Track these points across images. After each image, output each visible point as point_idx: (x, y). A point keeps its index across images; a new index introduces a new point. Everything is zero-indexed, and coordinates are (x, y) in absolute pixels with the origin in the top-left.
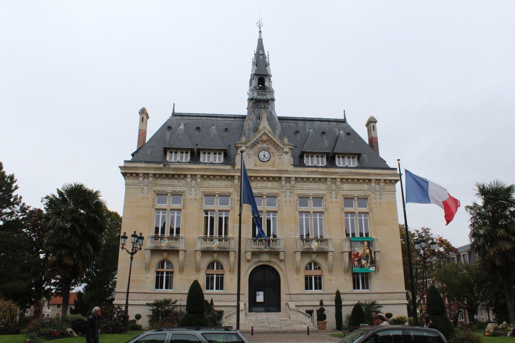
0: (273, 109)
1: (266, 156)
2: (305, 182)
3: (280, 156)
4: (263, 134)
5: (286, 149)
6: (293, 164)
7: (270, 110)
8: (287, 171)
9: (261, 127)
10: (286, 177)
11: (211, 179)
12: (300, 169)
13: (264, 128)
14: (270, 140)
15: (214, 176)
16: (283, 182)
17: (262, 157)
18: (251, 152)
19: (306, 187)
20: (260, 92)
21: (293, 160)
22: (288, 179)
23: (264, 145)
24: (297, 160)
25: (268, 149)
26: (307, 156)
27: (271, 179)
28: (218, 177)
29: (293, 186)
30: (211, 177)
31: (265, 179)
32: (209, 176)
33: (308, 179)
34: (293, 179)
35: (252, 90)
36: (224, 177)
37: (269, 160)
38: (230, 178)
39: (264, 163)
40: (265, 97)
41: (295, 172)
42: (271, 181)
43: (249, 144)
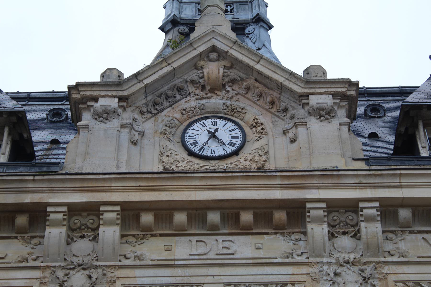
3: (291, 135)
4: (205, 56)
8: (331, 176)
10: (333, 206)
16: (318, 231)
17: (203, 138)
18: (148, 126)
22: (344, 215)
23: (214, 102)
25: (233, 111)
27: (247, 217)
29: (374, 249)
37: (236, 153)
38: (22, 220)
42: (247, 231)
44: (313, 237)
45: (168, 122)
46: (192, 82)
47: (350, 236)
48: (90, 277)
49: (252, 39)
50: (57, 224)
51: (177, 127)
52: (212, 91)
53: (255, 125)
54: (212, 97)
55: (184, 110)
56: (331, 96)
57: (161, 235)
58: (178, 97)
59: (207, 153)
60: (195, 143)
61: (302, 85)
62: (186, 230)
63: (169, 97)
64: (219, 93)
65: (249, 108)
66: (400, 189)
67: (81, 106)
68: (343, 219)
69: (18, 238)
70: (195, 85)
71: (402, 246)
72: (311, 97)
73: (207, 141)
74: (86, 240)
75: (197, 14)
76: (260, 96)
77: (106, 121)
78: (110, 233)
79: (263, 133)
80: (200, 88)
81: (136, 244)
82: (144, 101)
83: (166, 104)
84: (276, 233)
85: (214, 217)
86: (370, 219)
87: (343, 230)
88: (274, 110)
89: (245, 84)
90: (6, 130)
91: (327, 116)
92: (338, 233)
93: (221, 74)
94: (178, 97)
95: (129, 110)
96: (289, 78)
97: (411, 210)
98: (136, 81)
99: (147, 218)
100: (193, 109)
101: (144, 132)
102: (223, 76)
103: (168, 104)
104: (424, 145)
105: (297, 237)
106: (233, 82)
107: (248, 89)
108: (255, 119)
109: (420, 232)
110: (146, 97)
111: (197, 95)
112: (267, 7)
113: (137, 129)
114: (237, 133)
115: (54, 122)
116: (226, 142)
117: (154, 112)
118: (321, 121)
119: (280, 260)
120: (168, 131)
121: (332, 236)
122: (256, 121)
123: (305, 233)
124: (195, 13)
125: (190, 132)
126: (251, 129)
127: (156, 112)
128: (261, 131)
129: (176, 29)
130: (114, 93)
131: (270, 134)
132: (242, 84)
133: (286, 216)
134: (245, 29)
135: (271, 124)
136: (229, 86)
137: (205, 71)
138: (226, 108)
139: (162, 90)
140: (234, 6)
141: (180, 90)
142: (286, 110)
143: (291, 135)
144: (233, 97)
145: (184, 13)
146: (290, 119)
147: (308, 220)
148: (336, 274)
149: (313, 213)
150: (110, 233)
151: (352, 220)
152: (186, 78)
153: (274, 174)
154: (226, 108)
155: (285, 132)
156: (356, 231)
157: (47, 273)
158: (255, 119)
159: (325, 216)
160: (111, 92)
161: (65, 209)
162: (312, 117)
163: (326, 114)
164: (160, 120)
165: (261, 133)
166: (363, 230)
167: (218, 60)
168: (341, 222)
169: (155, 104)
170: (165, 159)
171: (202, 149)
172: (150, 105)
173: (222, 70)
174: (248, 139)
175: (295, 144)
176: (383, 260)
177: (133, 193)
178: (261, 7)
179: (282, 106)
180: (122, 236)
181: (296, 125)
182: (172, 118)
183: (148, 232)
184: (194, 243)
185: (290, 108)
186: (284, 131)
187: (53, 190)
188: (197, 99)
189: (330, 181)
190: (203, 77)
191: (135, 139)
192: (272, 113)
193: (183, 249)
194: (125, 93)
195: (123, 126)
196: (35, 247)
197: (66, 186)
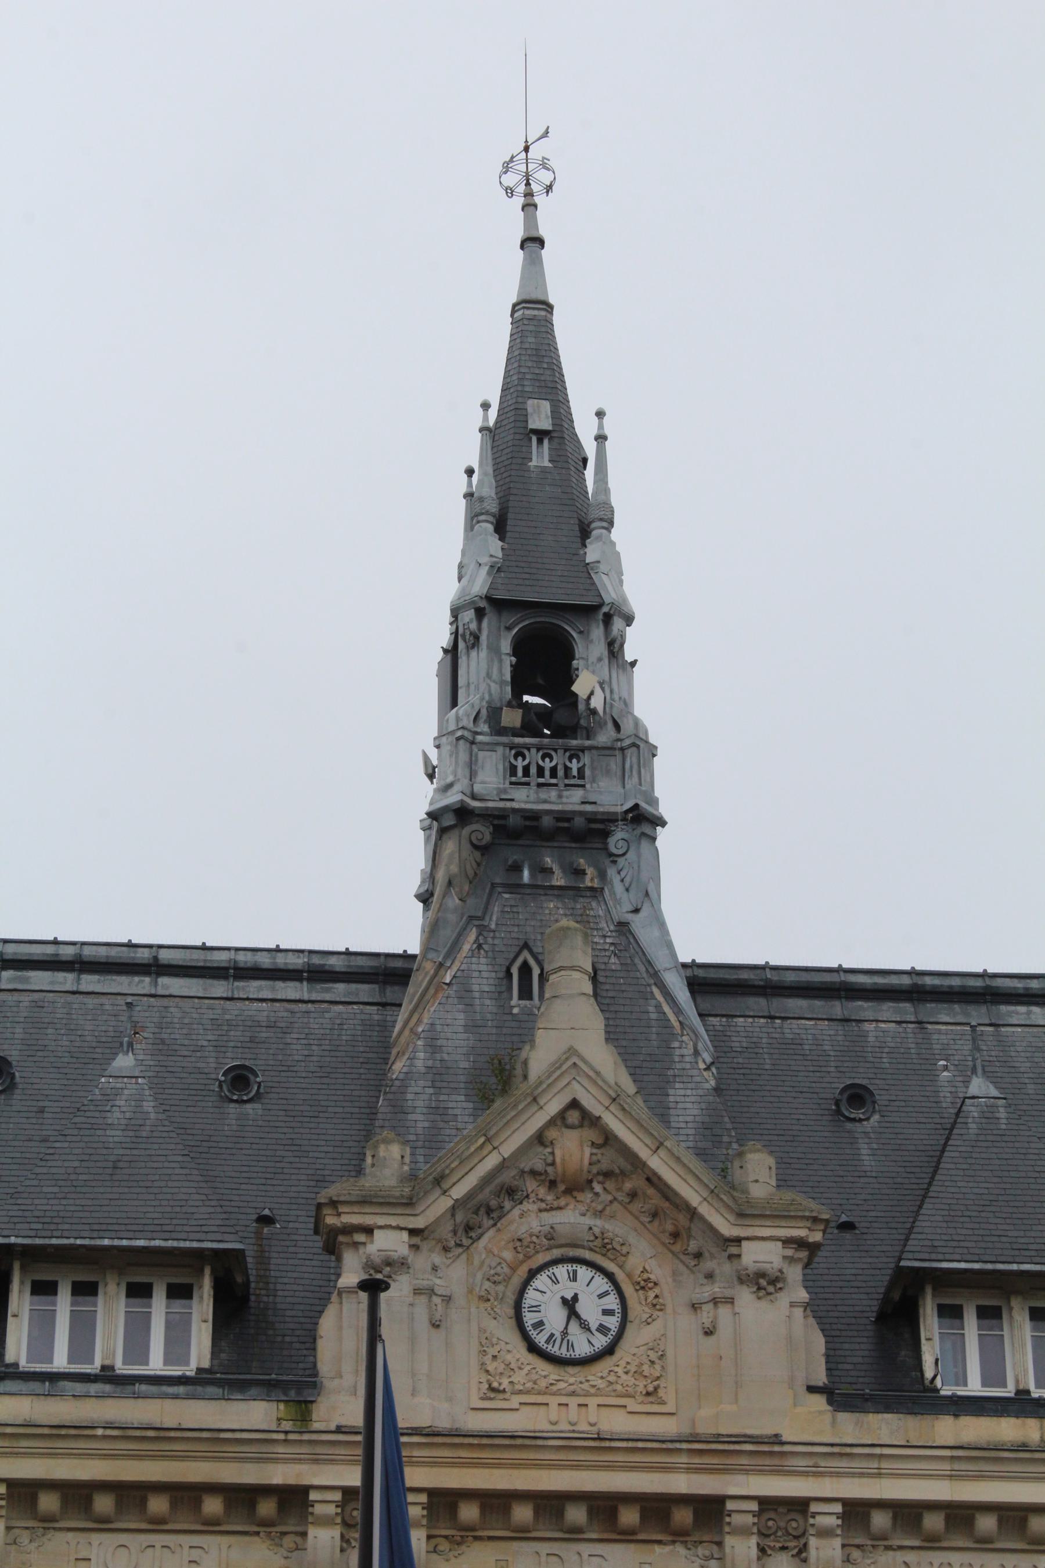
0: (647, 896)
1: (590, 1310)
3: (706, 1315)
5: (762, 1253)
6: (821, 1378)
7: (621, 911)
8: (770, 1451)
10: (767, 1504)
11: (103, 1524)
12: (884, 1427)
13: (571, 1061)
14: (619, 1173)
15: (131, 1495)
17: (555, 1318)
18: (455, 1275)
20: (534, 757)
21: (819, 1343)
23: (572, 1218)
24: (861, 1348)
25: (606, 1247)
26: (951, 1313)
27: (629, 1516)
28: (158, 1505)
30: (104, 1504)
31: (576, 1514)
32: (77, 1495)
33: (960, 1516)
34: (828, 1517)
35: (459, 739)
36: (213, 1506)
37: (609, 1351)
38: (267, 1508)
39: (572, 1376)
40: (572, 800)
42: (627, 1536)
43: (435, 1208)
44: (733, 1561)
45: (492, 1272)
46: (534, 1173)
47: (790, 1554)
49: (623, 874)
50: (326, 1521)
51: (507, 1279)
52: (568, 1192)
53: (644, 1285)
54: (567, 1205)
55: (520, 1240)
56: (780, 1244)
57: (491, 1538)
58: (507, 1204)
60: (539, 1325)
61: (731, 1218)
62: (529, 1532)
63: (492, 1211)
64: (580, 1196)
65: (632, 1239)
66: (877, 1480)
67: (341, 1238)
68: (782, 1524)
69: (262, 1534)
70: (538, 1178)
72: (744, 1243)
75: (507, 785)
76: (655, 1215)
80: (547, 1184)
81: (451, 1554)
82: (449, 1227)
83: (487, 1222)
84: (674, 1542)
86: (825, 1533)
87: (780, 1545)
88: (677, 1248)
90: (207, 1271)
91: (771, 1289)
92: (773, 1548)
93: (586, 1162)
94: (507, 1204)
95: (425, 1246)
96: (709, 1199)
97: (891, 1515)
98: (437, 1192)
99: (469, 1512)
100: (534, 1239)
101: (450, 1297)
102: (590, 1164)
103: (491, 1222)
104: (929, 1335)
105: (707, 1553)
106: (607, 1175)
107: (633, 1195)
108: (644, 1271)
109: (901, 1548)
110: (453, 1215)
111: (542, 1200)
112: (654, 755)
114: (612, 1302)
115: (236, 1101)
116: (594, 1326)
117: (466, 1242)
118: (759, 1298)
120: (493, 1293)
121: (762, 1550)
122: (645, 1276)
123: (720, 1544)
124: (505, 778)
125: (531, 1296)
126: (637, 1290)
127: (470, 1241)
128: (655, 1302)
129: (466, 831)
131: (669, 1309)
132: (623, 1182)
133: (691, 1516)
134: (606, 834)
135: (670, 1280)
136: (599, 1183)
137: (558, 1153)
138: (592, 1238)
139: (480, 1197)
140: (586, 759)
141: (511, 1192)
142: (698, 1255)
144: (604, 1209)
145: (480, 777)
146: (706, 1277)
147: (727, 1529)
151: (795, 1529)
152: (522, 1166)
153: (678, 1445)
154: (592, 1238)
156: (801, 1546)
158: (644, 1271)
159: (754, 1524)
160: (396, 1217)
161: (337, 1496)
162: (745, 1287)
163: (769, 1283)
164: (476, 1262)
165: (654, 1305)
166: (813, 1553)
167: (581, 1126)
168: (779, 1528)
169: (468, 1228)
173: (588, 1151)
174: (631, 1316)
175: (712, 1339)
177: (448, 1470)
178: (642, 770)
179: (693, 1246)
181: (715, 1301)
182: (498, 1260)
184: (543, 1558)
185: (707, 1254)
186: (693, 1305)
187: (317, 1460)
188: (540, 1211)
189: (768, 1461)
190: (553, 1164)
191: (437, 1317)
192: (673, 1253)
194: (419, 1223)
195: (417, 1291)
196: (289, 1554)
197: (337, 1452)
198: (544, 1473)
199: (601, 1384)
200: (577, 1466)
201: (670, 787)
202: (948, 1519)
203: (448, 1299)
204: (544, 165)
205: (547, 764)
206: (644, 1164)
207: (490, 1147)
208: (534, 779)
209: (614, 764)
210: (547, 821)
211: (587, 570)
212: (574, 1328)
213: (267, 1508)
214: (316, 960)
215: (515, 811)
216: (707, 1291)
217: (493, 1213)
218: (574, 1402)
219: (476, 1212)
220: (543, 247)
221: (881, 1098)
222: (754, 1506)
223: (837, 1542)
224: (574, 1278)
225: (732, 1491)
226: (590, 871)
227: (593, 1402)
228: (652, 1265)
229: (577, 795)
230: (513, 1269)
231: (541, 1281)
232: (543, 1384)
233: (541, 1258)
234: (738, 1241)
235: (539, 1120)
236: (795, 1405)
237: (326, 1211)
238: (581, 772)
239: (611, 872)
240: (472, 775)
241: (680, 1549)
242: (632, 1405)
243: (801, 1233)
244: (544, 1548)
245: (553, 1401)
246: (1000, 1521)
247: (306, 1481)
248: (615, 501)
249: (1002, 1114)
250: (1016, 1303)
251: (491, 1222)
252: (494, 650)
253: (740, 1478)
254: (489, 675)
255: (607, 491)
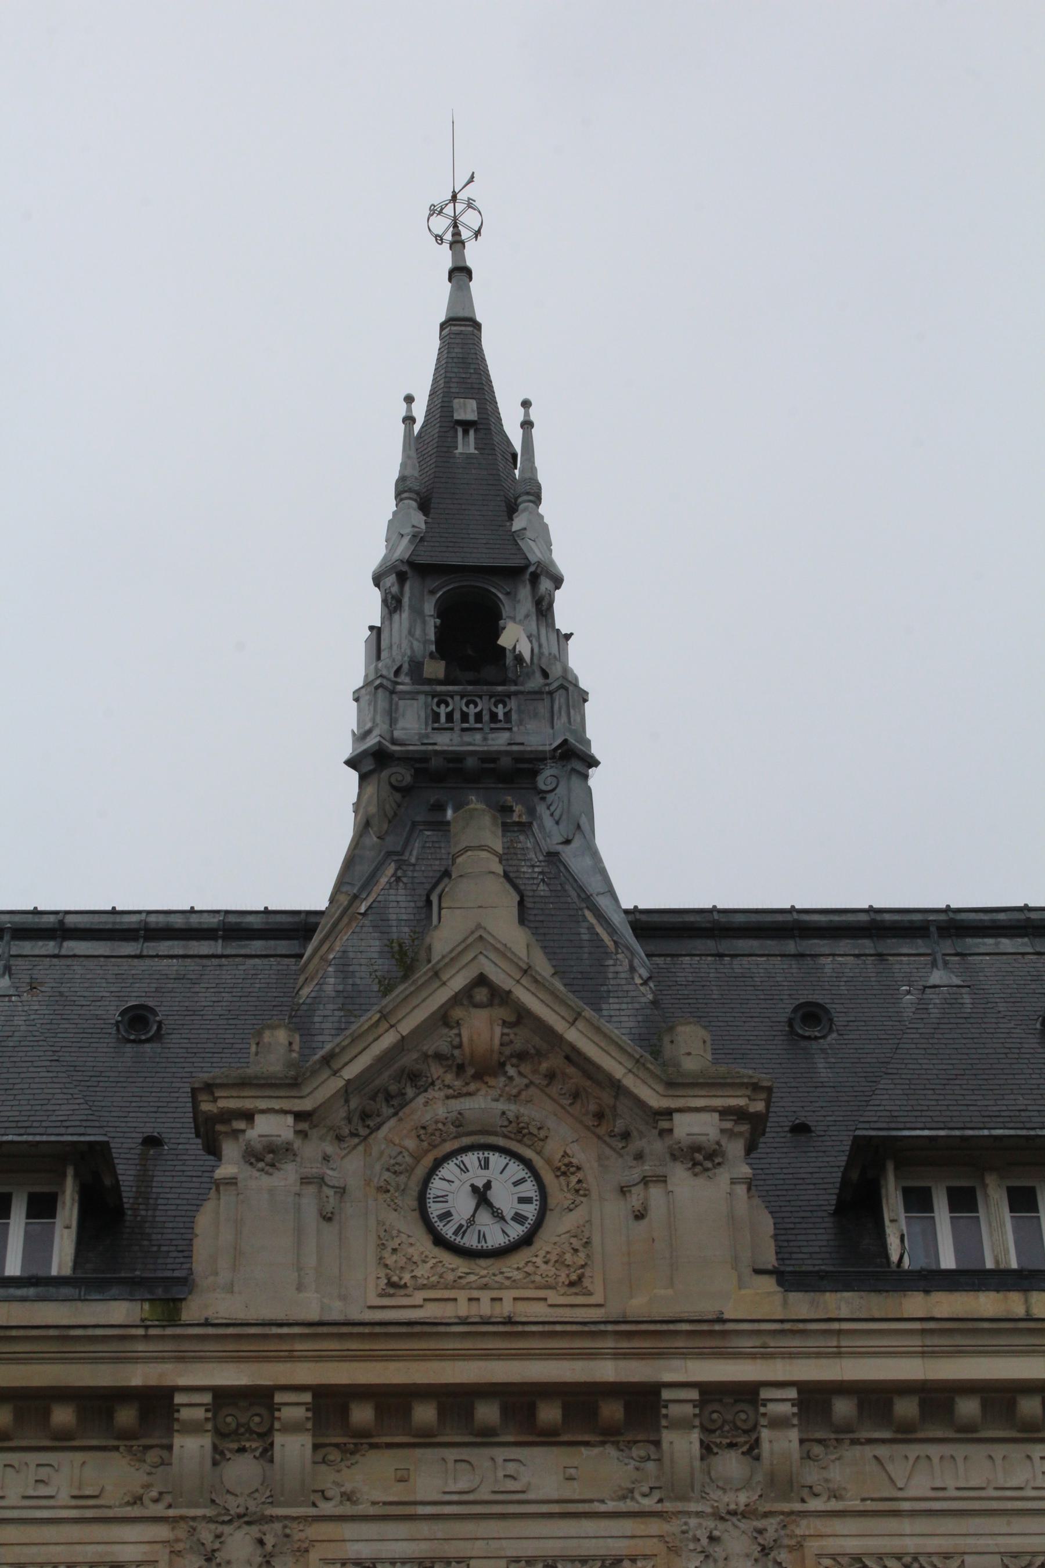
0: (580, 826)
1: (504, 1197)
2: (905, 1433)
3: (635, 1199)
5: (696, 1125)
7: (553, 843)
9: (446, 935)
10: (711, 1393)
12: (841, 1303)
13: (479, 939)
14: (534, 1052)
16: (682, 1445)
17: (463, 1205)
18: (351, 1167)
19: (920, 1485)
20: (457, 704)
21: (767, 1224)
22: (728, 1410)
23: (482, 1104)
24: (818, 1244)
25: (521, 1131)
26: (918, 1201)
27: (549, 1413)
29: (783, 1484)
31: (487, 1413)
33: (937, 1399)
35: (381, 689)
36: (63, 1416)
37: (527, 1240)
38: (126, 1416)
39: (484, 1268)
40: (499, 741)
41: (793, 1328)
42: (548, 1437)
43: (325, 1089)
44: (672, 1461)
45: (392, 1161)
46: (439, 1057)
47: (740, 1451)
48: (261, 1542)
49: (552, 808)
50: (193, 1428)
52: (478, 1076)
53: (566, 1169)
54: (478, 1090)
55: (424, 1128)
56: (716, 1115)
57: (389, 1446)
58: (410, 1092)
59: (470, 1241)
60: (446, 1216)
61: (660, 1088)
62: (435, 1436)
63: (392, 1097)
64: (492, 1081)
65: (551, 1123)
66: (837, 1360)
67: (219, 1128)
68: (729, 1417)
69: (122, 1449)
70: (445, 1063)
71: (837, 1474)
72: (676, 1117)
73: (473, 1216)
74: (248, 1457)
75: (429, 730)
76: (576, 1096)
77: (271, 1170)
78: (293, 1448)
79: (580, 1191)
80: (454, 1069)
81: (343, 1464)
82: (342, 1113)
83: (387, 1111)
84: (603, 1443)
85: (487, 1413)
86: (779, 1423)
87: (728, 1441)
88: (602, 1131)
89: (544, 1066)
90: (70, 1172)
92: (719, 1445)
93: (497, 1041)
94: (410, 1092)
95: (314, 1134)
96: (635, 1070)
97: (855, 1401)
98: (326, 1073)
99: (362, 1414)
100: (440, 1126)
101: (344, 1189)
102: (502, 1045)
103: (392, 1111)
104: (893, 1216)
105: (643, 1453)
106: (522, 1056)
107: (551, 1076)
108: (565, 1154)
109: (870, 1441)
110: (347, 1101)
111: (449, 1087)
112: (585, 701)
113: (331, 1184)
114: (529, 1189)
115: (133, 1041)
116: (508, 1214)
117: (363, 1132)
118: (696, 1175)
119: (611, 1506)
120: (393, 1184)
121: (707, 1449)
122: (566, 1160)
123: (657, 1444)
124: (427, 724)
125: (437, 1186)
126: (557, 1177)
127: (367, 1131)
128: (577, 1187)
129: (385, 774)
130: (286, 1104)
131: (594, 1195)
132: (540, 1063)
133: (622, 1410)
134: (535, 773)
135: (595, 1165)
136: (512, 1066)
138: (506, 1123)
139: (377, 1082)
140: (513, 704)
141: (413, 1077)
142: (626, 1136)
143: (635, 1199)
144: (519, 1093)
145: (401, 724)
146: (635, 1159)
147: (664, 1423)
148: (712, 1539)
149: (674, 1410)
150: (293, 1448)
151: (745, 1421)
152: (425, 1048)
153: (602, 1327)
154: (506, 1123)
155: (624, 1191)
156: (752, 1441)
157: (181, 1532)
158: (565, 1154)
159: (695, 1415)
160: (280, 1100)
161: (207, 1398)
162: (678, 1164)
163: (706, 1158)
164: (375, 1152)
165: (577, 1191)
166: (765, 1446)
167: (490, 1004)
168: (725, 1422)
169: (365, 1116)
170: (390, 1260)
171: (459, 1230)
172: (356, 1119)
173: (498, 1030)
174: (552, 1202)
175: (644, 1222)
176: (798, 1506)
177: (336, 1364)
178: (572, 712)
179: (620, 1125)
180: (316, 1447)
181: (645, 1181)
182: (399, 1149)
183: (361, 1442)
184: (451, 1465)
185: (635, 1133)
186: (622, 1187)
187: (183, 1358)
188: (448, 1097)
190: (460, 1046)
191: (329, 1208)
192: (599, 1137)
193: (432, 1477)
194: (307, 1105)
195: (305, 1181)
196: (154, 1470)
197: (206, 1349)
198: (448, 1365)
199: (517, 1275)
200: (487, 1355)
201: (600, 728)
202: (922, 1404)
203: (342, 1191)
204: (470, 204)
205: (472, 710)
206: (560, 1038)
207: (387, 1026)
208: (458, 725)
209: (542, 708)
210: (471, 763)
211: (514, 539)
212: (484, 1217)
213: (126, 1416)
214: (232, 919)
215: (436, 752)
216: (636, 1175)
217: (396, 1101)
218: (485, 1296)
219: (373, 1098)
220: (471, 279)
221: (839, 1020)
222: (694, 1394)
223: (794, 1435)
224: (485, 1165)
225: (667, 1377)
226: (518, 808)
227: (508, 1295)
228: (574, 1149)
229: (505, 736)
230: (417, 1160)
231: (449, 1170)
232: (450, 1277)
233: (448, 1147)
234: (669, 1113)
235: (443, 996)
236: (740, 1288)
237: (202, 1097)
238: (507, 715)
239: (541, 809)
240: (392, 722)
241: (611, 1451)
242: (553, 1297)
243: (742, 1102)
244: (451, 1454)
245: (462, 1296)
246: (984, 1405)
247: (169, 1382)
248: (541, 478)
249: (967, 999)
250: (991, 1180)
251: (392, 1111)
252: (417, 612)
253: (676, 1363)
254: (411, 633)
255: (533, 469)
